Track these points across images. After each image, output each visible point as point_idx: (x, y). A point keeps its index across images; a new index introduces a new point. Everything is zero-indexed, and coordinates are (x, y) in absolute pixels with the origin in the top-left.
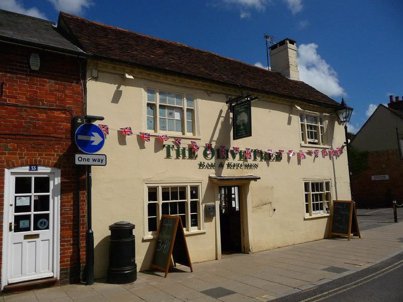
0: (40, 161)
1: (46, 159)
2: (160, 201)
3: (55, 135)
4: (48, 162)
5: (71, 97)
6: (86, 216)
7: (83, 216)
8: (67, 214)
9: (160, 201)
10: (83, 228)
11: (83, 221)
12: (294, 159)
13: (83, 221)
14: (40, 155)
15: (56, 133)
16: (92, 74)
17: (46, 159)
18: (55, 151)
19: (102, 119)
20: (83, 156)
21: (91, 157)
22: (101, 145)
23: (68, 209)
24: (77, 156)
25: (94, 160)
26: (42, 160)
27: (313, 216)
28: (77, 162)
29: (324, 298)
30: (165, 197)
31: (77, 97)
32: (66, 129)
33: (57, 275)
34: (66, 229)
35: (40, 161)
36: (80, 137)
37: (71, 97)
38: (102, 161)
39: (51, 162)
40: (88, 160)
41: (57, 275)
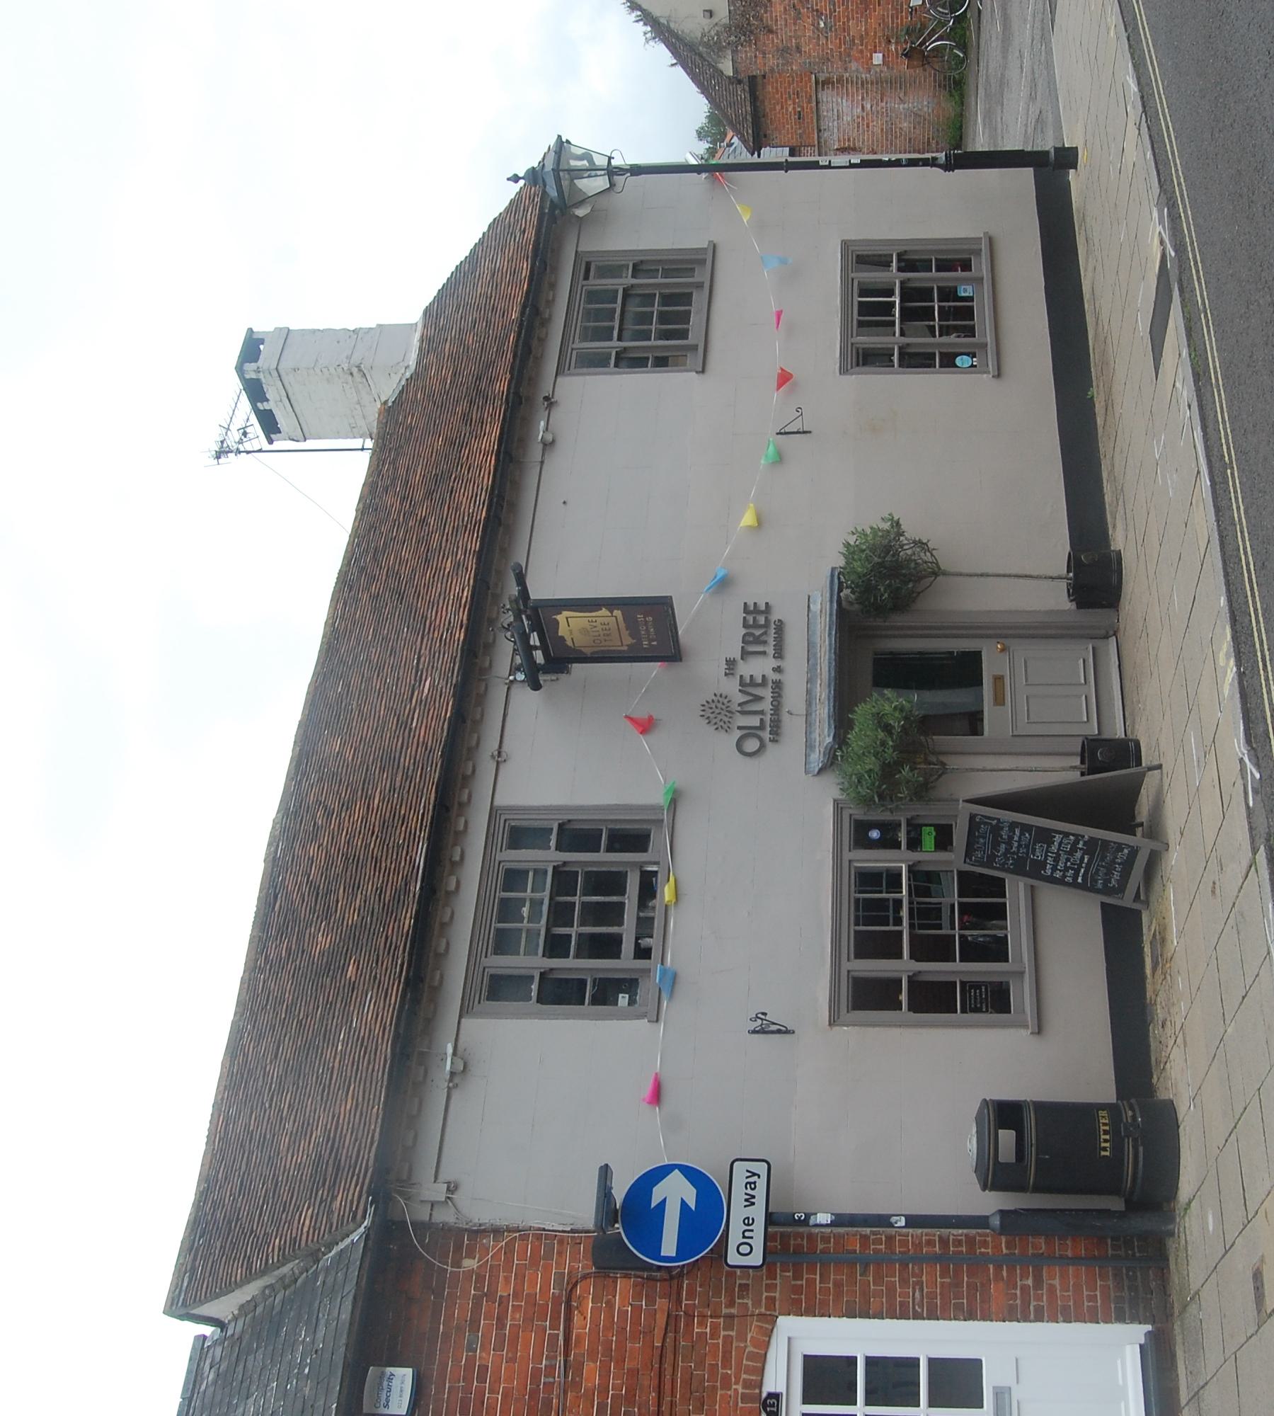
0: (747, 1385)
1: (739, 1363)
2: (903, 967)
3: (658, 1333)
4: (752, 1357)
5: (520, 1278)
6: (945, 1231)
7: (944, 1242)
8: (932, 1296)
9: (903, 967)
10: (984, 1244)
11: (959, 1243)
12: (702, 713)
13: (958, 1243)
14: (726, 1383)
15: (650, 1332)
16: (442, 1202)
17: (739, 1363)
18: (714, 1334)
19: (605, 1172)
20: (735, 1238)
21: (738, 1212)
22: (691, 1174)
23: (917, 1294)
24: (733, 1258)
25: (750, 1201)
26: (744, 1376)
27: (989, 339)
28: (756, 1259)
29: (1227, 423)
30: (889, 947)
31: (522, 1256)
32: (638, 1296)
33: (1138, 1332)
34: (982, 1302)
35: (747, 1385)
36: (669, 1246)
37: (520, 1278)
38: (754, 1174)
39: (750, 1349)
40: (748, 1222)
41: (1138, 1332)
